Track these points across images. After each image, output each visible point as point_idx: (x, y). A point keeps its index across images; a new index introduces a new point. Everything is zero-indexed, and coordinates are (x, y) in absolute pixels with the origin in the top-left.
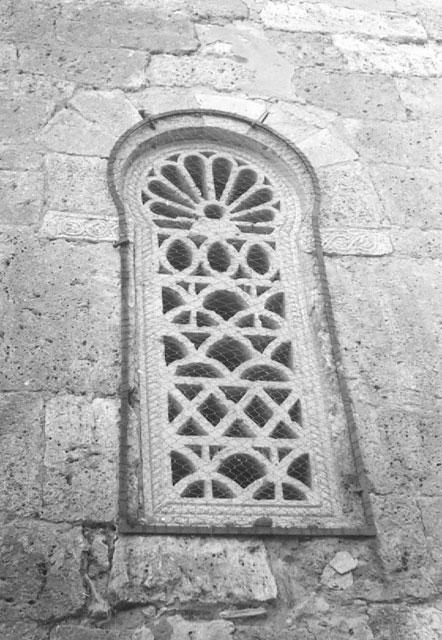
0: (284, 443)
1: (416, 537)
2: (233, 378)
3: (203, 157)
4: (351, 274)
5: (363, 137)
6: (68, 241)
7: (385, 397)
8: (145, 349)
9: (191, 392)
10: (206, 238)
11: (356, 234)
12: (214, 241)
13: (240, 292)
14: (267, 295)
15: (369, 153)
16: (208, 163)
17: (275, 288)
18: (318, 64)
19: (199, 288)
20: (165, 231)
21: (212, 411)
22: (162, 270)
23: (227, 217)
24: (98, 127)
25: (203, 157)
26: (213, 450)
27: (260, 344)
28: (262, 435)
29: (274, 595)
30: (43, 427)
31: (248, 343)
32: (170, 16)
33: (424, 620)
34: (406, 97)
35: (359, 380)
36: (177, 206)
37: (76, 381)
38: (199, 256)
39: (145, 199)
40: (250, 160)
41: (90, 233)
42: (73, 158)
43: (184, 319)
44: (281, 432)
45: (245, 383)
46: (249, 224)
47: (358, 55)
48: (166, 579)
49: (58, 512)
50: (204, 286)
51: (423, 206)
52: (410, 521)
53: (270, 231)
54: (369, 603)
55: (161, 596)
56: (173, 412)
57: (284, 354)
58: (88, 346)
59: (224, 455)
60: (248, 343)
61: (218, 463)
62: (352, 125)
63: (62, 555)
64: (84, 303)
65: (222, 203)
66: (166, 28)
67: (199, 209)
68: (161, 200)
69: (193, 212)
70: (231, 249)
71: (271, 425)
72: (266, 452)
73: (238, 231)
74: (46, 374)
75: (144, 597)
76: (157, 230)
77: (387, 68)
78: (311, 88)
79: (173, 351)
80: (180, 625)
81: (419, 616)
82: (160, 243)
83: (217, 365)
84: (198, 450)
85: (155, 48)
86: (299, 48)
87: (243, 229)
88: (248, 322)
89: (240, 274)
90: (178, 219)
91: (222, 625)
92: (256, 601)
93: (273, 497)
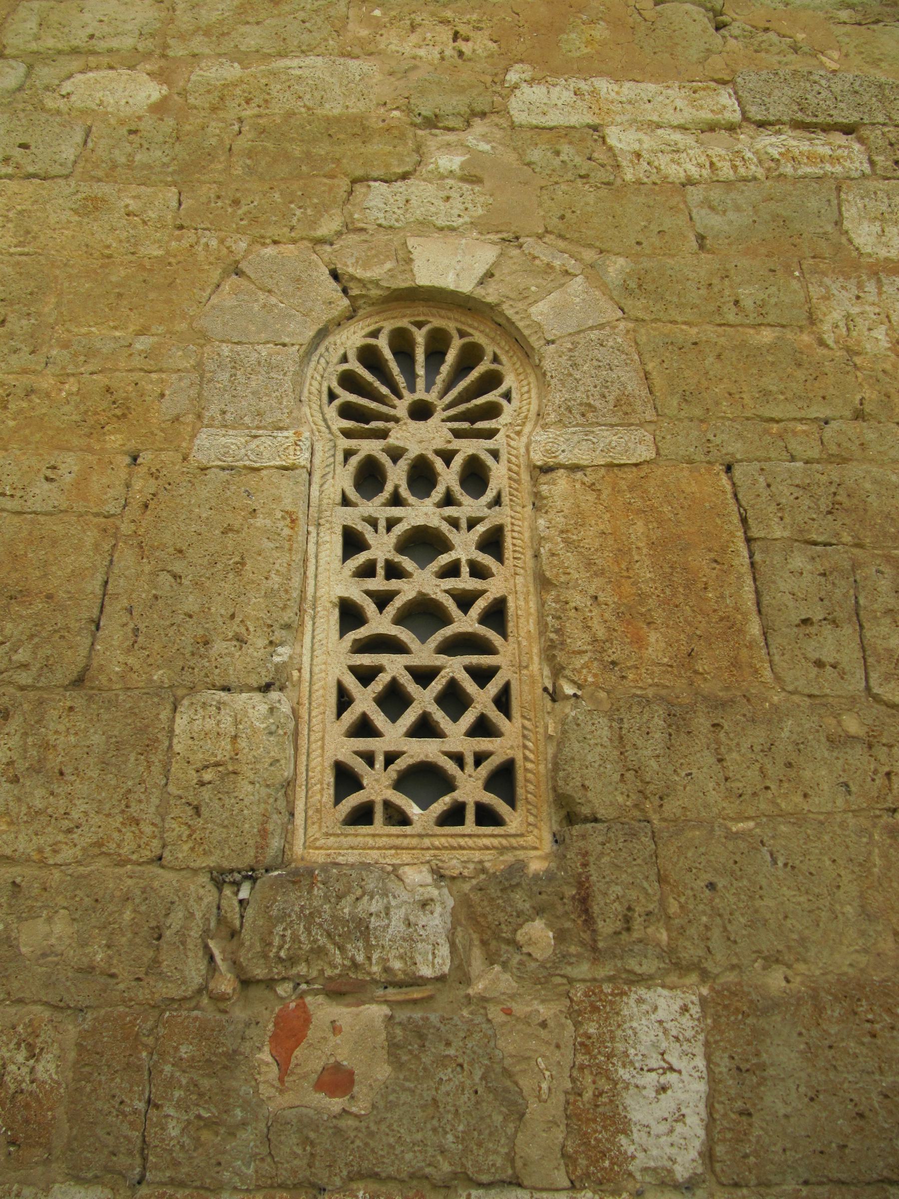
0: (484, 744)
1: (646, 885)
3: (414, 329)
4: (595, 494)
5: (633, 285)
6: (223, 469)
7: (623, 677)
8: (314, 618)
9: (365, 676)
10: (407, 450)
11: (606, 434)
12: (417, 453)
13: (445, 527)
14: (480, 529)
15: (637, 307)
16: (420, 337)
17: (494, 517)
18: (581, 177)
19: (391, 524)
20: (352, 443)
22: (346, 502)
23: (439, 415)
24: (273, 300)
25: (414, 329)
26: (391, 758)
27: (465, 601)
29: (446, 969)
30: (171, 740)
31: (450, 604)
32: (384, 121)
33: (645, 1007)
35: (589, 654)
36: (373, 405)
37: (217, 671)
39: (332, 396)
40: (476, 329)
41: (252, 457)
42: (239, 348)
43: (367, 571)
45: (441, 659)
46: (465, 425)
47: (638, 156)
48: (306, 947)
49: (180, 856)
50: (398, 520)
51: (705, 384)
52: (639, 861)
53: (490, 434)
54: (571, 981)
55: (302, 969)
56: (344, 700)
58: (237, 620)
59: (401, 764)
60: (450, 604)
61: (394, 776)
63: (181, 915)
64: (237, 559)
65: (432, 397)
66: (375, 141)
67: (401, 408)
68: (353, 398)
69: (392, 412)
70: (439, 464)
71: (468, 718)
72: (458, 759)
73: (450, 435)
74: (181, 663)
75: (278, 971)
76: (345, 443)
77: (675, 172)
78: (568, 215)
81: (640, 1001)
82: (346, 459)
83: (404, 634)
84: (369, 758)
85: (359, 173)
86: (558, 153)
87: (458, 434)
88: (452, 570)
89: (449, 500)
90: (374, 425)
91: (376, 1012)
92: (421, 977)
93: (461, 822)
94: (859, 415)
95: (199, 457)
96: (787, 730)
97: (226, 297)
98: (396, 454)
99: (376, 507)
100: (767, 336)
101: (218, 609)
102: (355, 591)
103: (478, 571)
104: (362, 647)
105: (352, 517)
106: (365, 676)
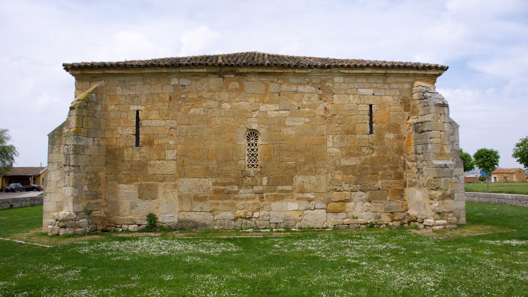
2: (253, 157)
17: (257, 148)
21: (251, 160)
28: (255, 162)
34: (274, 121)
38: (251, 145)
43: (249, 152)
44: (256, 162)
56: (248, 161)
57: (257, 155)
62: (267, 127)
67: (251, 139)
77: (273, 116)
79: (248, 155)
80: (247, 178)
88: (254, 152)
89: (254, 147)
91: (250, 178)
94: (283, 140)
95: (238, 143)
96: (274, 163)
97: (238, 130)
98: (251, 143)
99: (249, 147)
100: (277, 133)
101: (240, 155)
102: (248, 153)
103: (256, 152)
104: (249, 157)
105: (248, 148)
106: (249, 159)
